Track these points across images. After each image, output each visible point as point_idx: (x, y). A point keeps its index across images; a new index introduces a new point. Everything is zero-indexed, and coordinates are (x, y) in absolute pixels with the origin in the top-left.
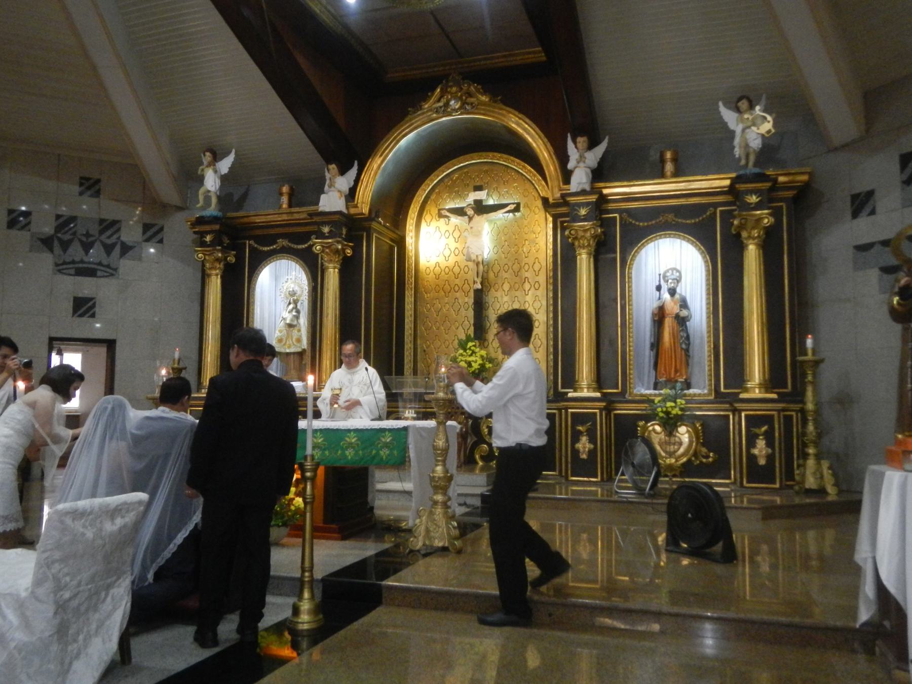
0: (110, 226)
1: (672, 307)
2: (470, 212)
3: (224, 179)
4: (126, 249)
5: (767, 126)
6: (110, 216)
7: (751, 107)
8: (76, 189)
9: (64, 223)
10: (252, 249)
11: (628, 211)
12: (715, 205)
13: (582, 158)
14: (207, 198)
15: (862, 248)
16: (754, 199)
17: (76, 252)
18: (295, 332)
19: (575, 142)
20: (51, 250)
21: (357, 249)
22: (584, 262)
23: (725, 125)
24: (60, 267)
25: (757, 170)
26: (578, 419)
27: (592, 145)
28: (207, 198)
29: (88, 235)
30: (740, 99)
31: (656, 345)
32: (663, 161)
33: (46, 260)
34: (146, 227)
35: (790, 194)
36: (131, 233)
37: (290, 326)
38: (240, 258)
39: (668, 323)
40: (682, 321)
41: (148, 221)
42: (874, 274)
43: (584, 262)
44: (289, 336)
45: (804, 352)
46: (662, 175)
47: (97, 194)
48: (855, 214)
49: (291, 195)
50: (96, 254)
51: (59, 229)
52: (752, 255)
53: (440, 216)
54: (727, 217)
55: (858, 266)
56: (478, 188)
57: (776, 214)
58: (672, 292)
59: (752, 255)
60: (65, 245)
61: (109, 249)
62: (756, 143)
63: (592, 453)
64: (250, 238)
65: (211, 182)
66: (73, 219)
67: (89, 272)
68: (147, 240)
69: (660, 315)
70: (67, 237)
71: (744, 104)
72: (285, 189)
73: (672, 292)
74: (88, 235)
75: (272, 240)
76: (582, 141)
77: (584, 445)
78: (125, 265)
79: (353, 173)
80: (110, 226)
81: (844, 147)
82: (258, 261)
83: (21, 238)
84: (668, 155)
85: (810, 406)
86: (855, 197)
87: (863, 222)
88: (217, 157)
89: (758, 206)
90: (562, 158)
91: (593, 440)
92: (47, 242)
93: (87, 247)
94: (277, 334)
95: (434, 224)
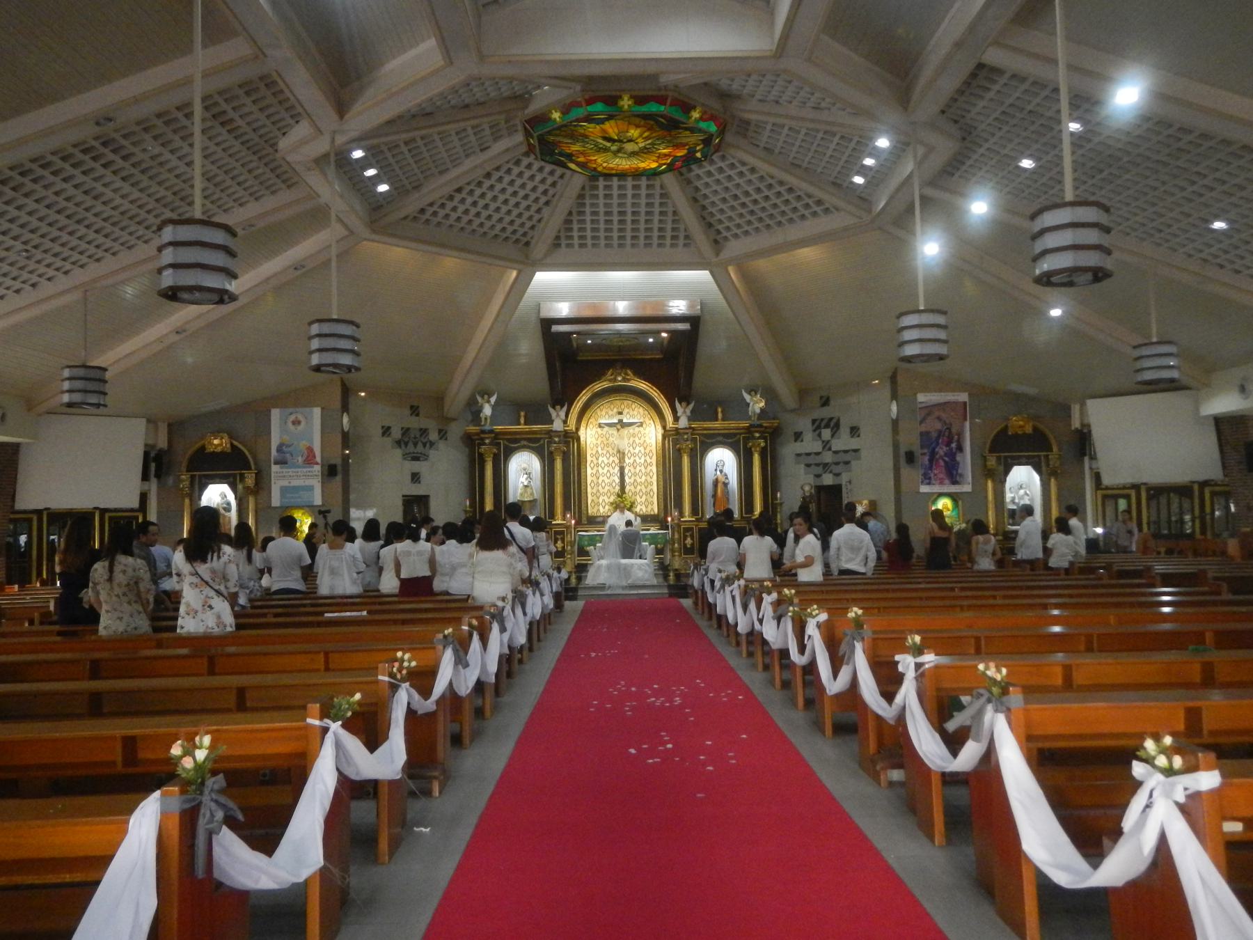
0: (424, 432)
1: (722, 479)
2: (619, 427)
3: (494, 408)
4: (432, 444)
5: (762, 404)
6: (423, 426)
7: (756, 394)
8: (407, 412)
9: (406, 431)
10: (506, 447)
11: (702, 434)
12: (741, 434)
13: (685, 412)
14: (486, 419)
15: (798, 455)
16: (757, 435)
17: (411, 448)
18: (529, 490)
19: (680, 403)
20: (400, 447)
21: (568, 447)
22: (686, 460)
23: (744, 399)
24: (405, 457)
25: (758, 423)
26: (686, 530)
27: (688, 404)
28: (486, 419)
29: (415, 438)
30: (752, 390)
31: (715, 496)
32: (717, 413)
33: (398, 453)
34: (440, 431)
35: (770, 431)
36: (433, 436)
37: (526, 486)
38: (499, 450)
39: (720, 487)
40: (725, 485)
41: (440, 427)
42: (803, 466)
43: (686, 460)
44: (526, 492)
45: (776, 499)
46: (716, 419)
47: (417, 415)
48: (796, 441)
49: (525, 417)
50: (420, 448)
51: (403, 434)
52: (756, 459)
53: (600, 426)
54: (746, 440)
55: (798, 463)
56: (620, 413)
57: (766, 442)
58: (721, 471)
59: (756, 459)
60: (406, 444)
61: (424, 444)
62: (758, 411)
63: (692, 545)
64: (503, 439)
65: (487, 411)
66: (408, 429)
67: (416, 459)
68: (441, 439)
69: (716, 483)
70: (406, 440)
71: (753, 393)
72: (522, 414)
73: (721, 471)
74: (415, 438)
75: (516, 441)
76: (684, 404)
77: (689, 541)
78: (432, 453)
79: (565, 408)
80: (424, 432)
81: (793, 411)
82: (509, 453)
83: (388, 441)
84: (720, 410)
85: (779, 521)
86: (795, 433)
87: (798, 444)
88: (490, 396)
89: (759, 438)
90: (674, 411)
91: (692, 539)
92: (398, 443)
93: (415, 445)
94: (520, 491)
95: (595, 429)
